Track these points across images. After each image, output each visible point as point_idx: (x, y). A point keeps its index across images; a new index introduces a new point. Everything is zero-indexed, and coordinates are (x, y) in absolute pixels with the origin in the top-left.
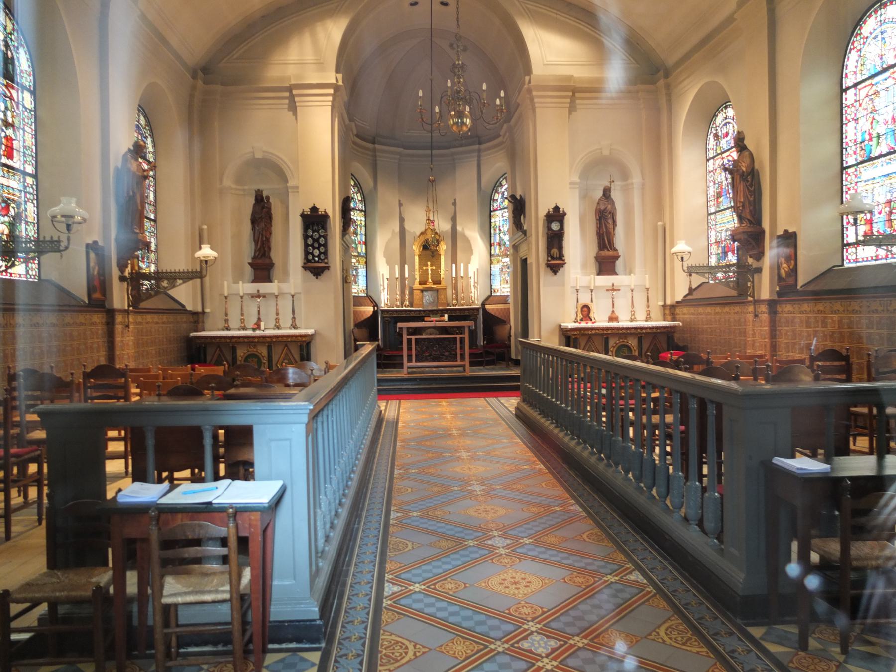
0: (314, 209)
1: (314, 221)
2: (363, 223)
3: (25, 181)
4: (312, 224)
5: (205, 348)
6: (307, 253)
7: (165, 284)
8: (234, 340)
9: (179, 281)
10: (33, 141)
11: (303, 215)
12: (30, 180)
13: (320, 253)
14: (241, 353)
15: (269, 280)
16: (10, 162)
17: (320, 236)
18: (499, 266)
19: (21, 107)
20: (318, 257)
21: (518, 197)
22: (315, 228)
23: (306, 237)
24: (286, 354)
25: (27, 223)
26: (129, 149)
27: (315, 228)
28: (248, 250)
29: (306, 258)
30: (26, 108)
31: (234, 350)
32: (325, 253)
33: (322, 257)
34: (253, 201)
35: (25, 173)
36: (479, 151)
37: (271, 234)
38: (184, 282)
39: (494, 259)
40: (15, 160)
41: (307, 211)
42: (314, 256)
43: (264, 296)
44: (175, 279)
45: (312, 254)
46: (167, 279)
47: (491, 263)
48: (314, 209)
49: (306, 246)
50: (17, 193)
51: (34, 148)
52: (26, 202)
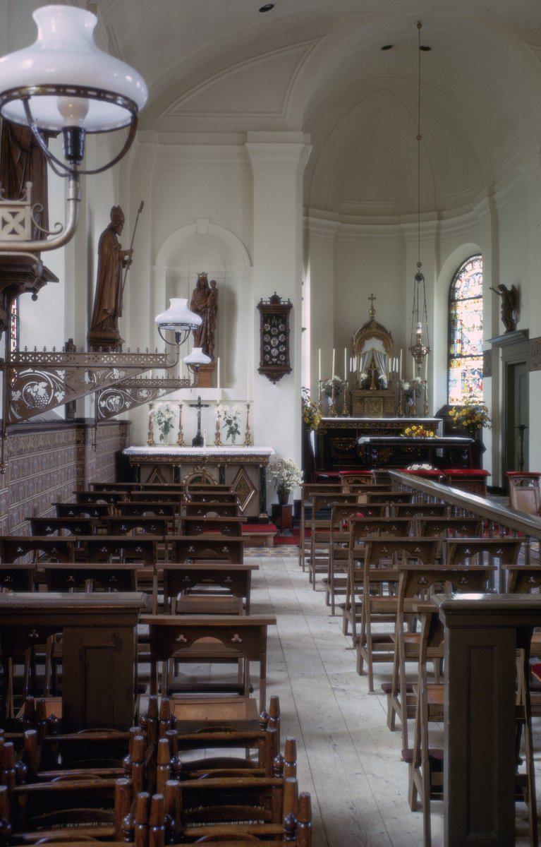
0: (275, 299)
1: (276, 316)
5: (139, 469)
7: (144, 393)
8: (178, 460)
9: (162, 391)
11: (261, 307)
13: (280, 353)
14: (186, 476)
15: (211, 384)
17: (280, 333)
18: (463, 367)
20: (277, 357)
21: (509, 288)
23: (264, 333)
24: (242, 479)
31: (177, 472)
36: (439, 227)
38: (167, 393)
39: (455, 362)
42: (272, 357)
43: (207, 406)
44: (157, 387)
45: (269, 353)
46: (147, 387)
47: (449, 365)
48: (275, 299)
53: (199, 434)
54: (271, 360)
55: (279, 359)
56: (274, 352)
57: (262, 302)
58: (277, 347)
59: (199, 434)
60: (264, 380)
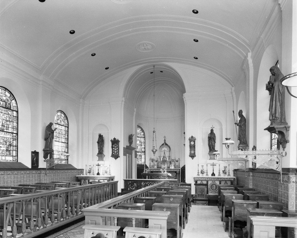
0: (115, 139)
1: (115, 142)
2: (144, 142)
3: (13, 135)
4: (115, 143)
6: (113, 152)
10: (17, 124)
12: (15, 135)
13: (117, 152)
16: (8, 131)
17: (117, 147)
19: (12, 116)
20: (116, 153)
22: (115, 144)
23: (112, 147)
25: (13, 146)
26: (48, 125)
27: (115, 144)
28: (97, 151)
29: (112, 154)
30: (14, 116)
32: (118, 152)
33: (117, 153)
34: (98, 137)
35: (13, 133)
37: (103, 146)
40: (9, 130)
41: (113, 139)
42: (115, 153)
45: (114, 152)
48: (115, 139)
49: (113, 150)
50: (10, 139)
51: (17, 126)
52: (13, 141)
53: (98, 172)
54: (115, 154)
55: (116, 154)
56: (116, 152)
57: (111, 140)
58: (116, 151)
59: (98, 172)
60: (113, 159)
